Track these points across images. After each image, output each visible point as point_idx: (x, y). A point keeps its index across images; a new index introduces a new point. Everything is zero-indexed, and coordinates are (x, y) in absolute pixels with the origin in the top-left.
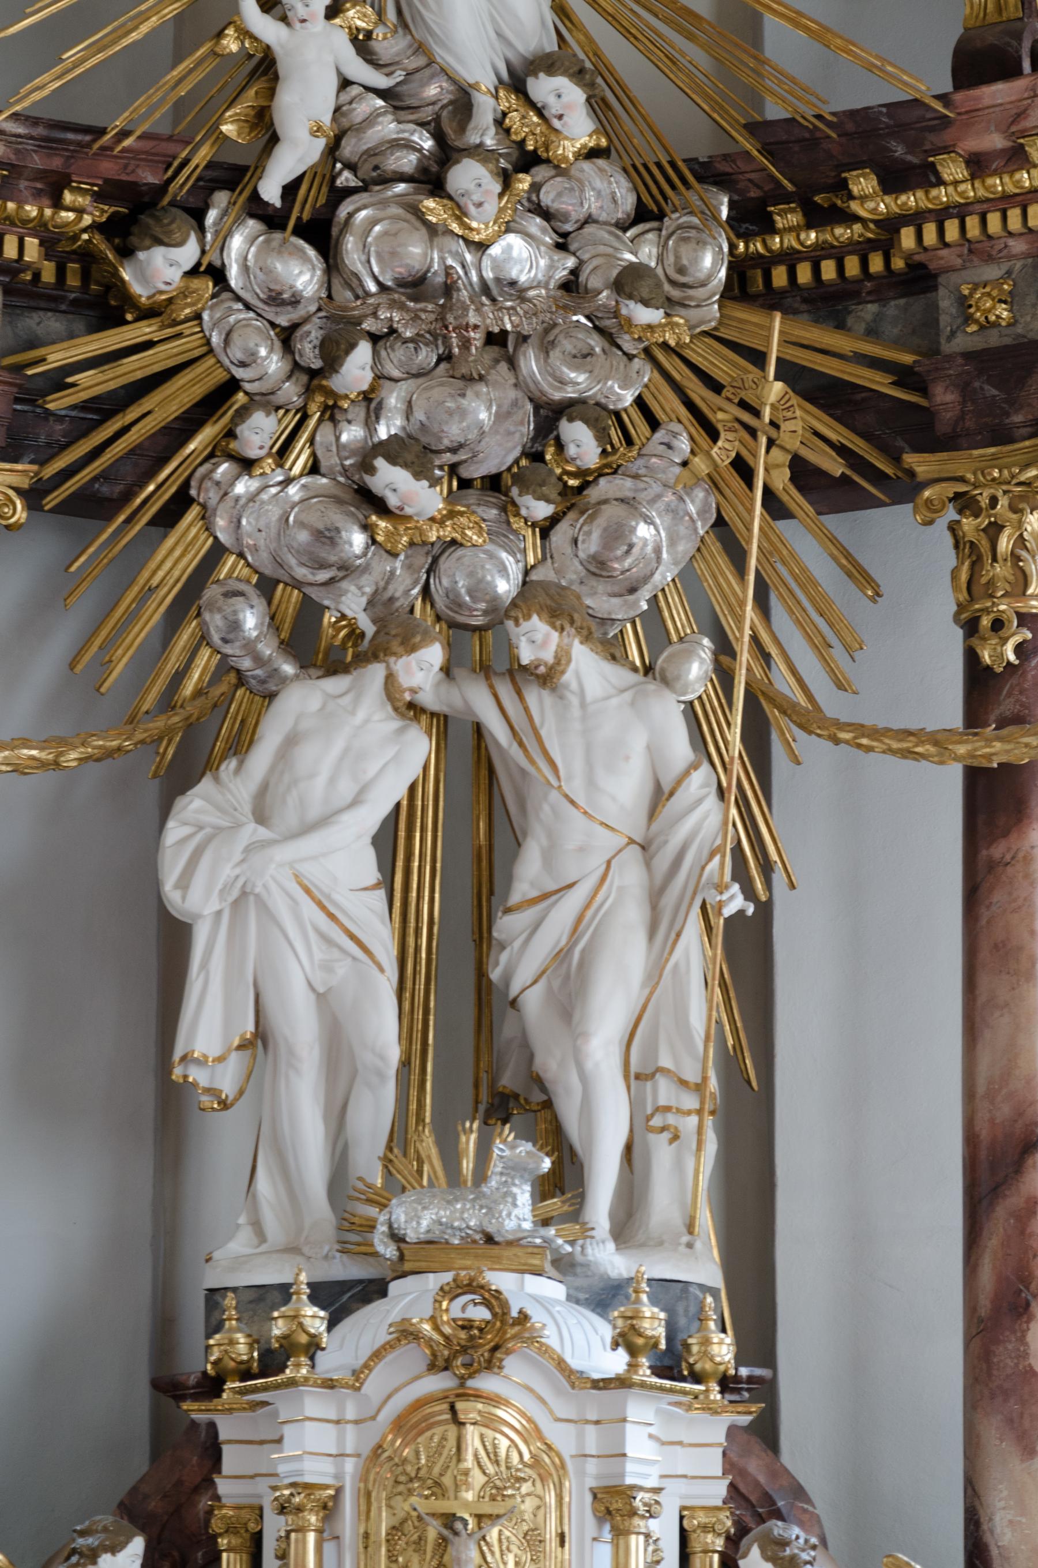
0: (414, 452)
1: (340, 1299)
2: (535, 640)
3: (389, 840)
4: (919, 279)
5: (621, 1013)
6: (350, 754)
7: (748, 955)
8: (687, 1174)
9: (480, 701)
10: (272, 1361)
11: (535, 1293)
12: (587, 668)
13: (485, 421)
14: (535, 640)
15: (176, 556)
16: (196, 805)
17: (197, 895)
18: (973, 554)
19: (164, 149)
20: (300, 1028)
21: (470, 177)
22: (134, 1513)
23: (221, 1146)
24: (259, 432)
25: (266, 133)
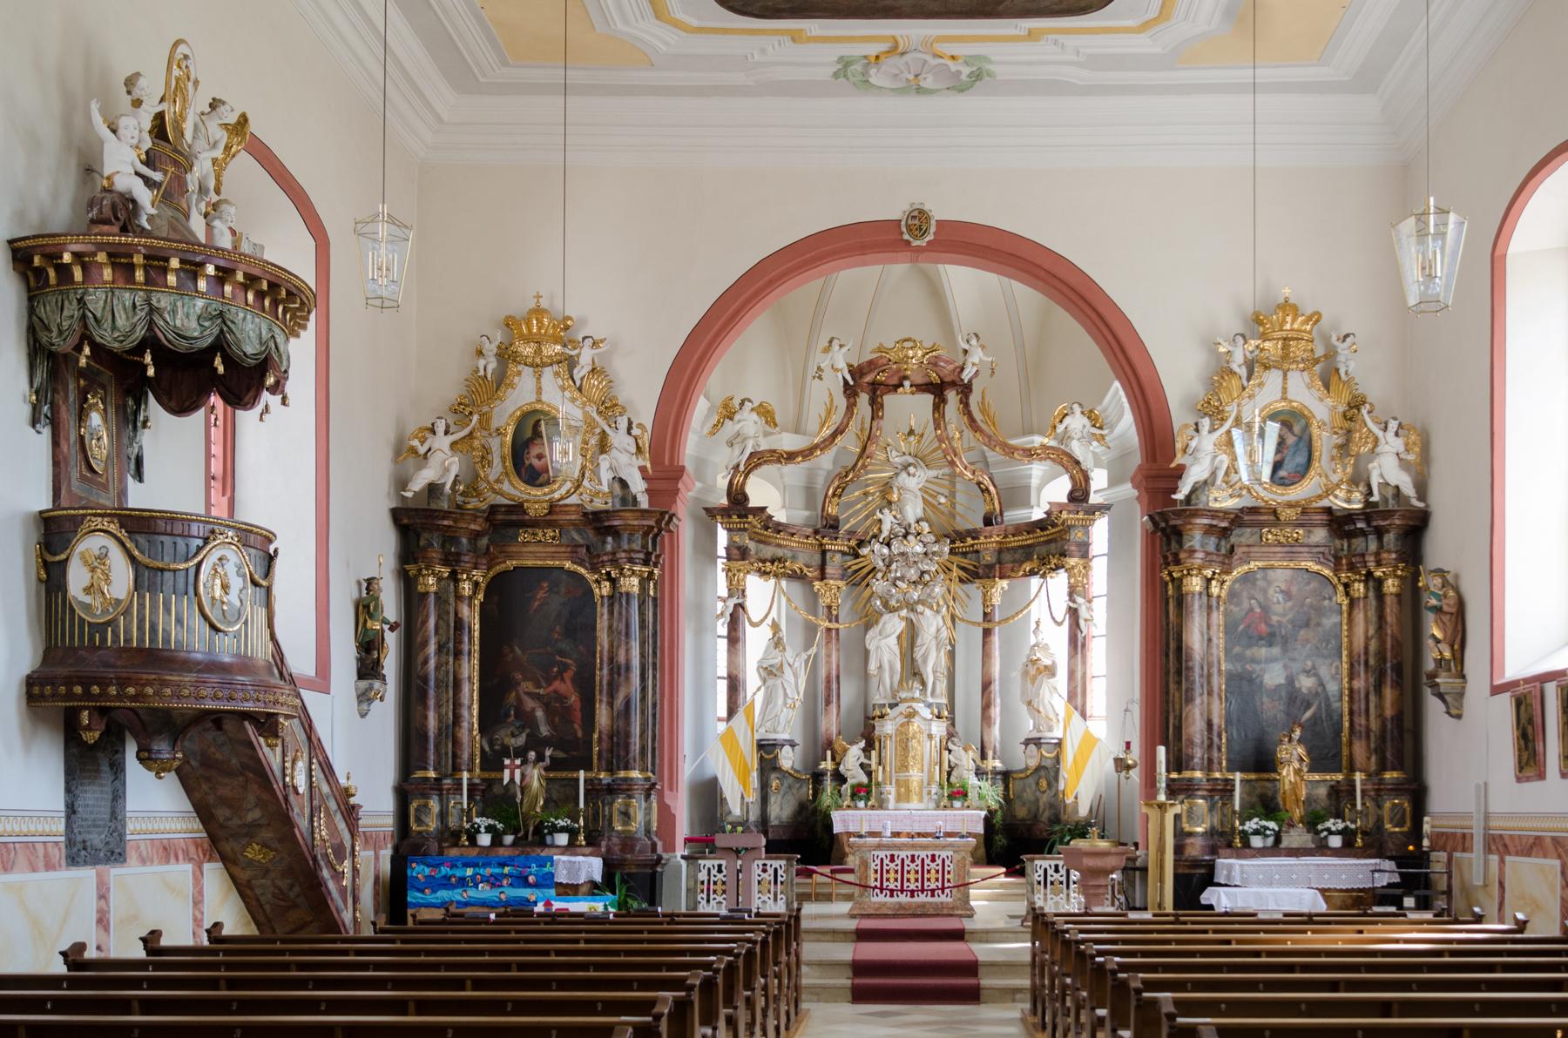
0: (902, 579)
1: (892, 706)
2: (920, 608)
3: (899, 638)
4: (977, 552)
5: (933, 662)
6: (893, 625)
7: (952, 655)
8: (942, 686)
9: (912, 616)
10: (882, 717)
11: (919, 707)
12: (928, 612)
13: (913, 574)
14: (920, 608)
15: (867, 592)
16: (871, 633)
17: (871, 647)
18: (985, 595)
19: (866, 532)
20: (886, 666)
21: (910, 537)
22: (863, 736)
23: (874, 682)
24: (879, 575)
25: (880, 530)
